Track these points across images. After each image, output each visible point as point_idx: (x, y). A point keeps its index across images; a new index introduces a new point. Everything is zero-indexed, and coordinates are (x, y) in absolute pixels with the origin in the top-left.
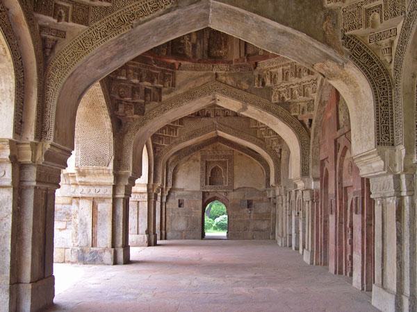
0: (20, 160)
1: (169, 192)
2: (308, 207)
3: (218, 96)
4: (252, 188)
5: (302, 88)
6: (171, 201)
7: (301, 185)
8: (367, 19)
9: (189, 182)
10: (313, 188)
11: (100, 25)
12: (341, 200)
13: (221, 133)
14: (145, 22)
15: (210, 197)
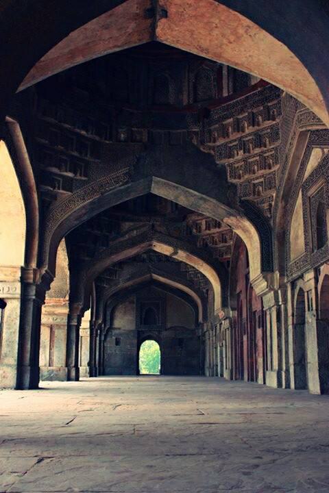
0: (25, 281)
1: (108, 331)
2: (228, 333)
3: (155, 243)
4: (183, 327)
5: (221, 236)
6: (108, 339)
7: (221, 314)
8: (254, 190)
9: (124, 322)
10: (231, 316)
11: (80, 192)
12: (251, 322)
13: (155, 276)
14: (111, 190)
15: (146, 335)
